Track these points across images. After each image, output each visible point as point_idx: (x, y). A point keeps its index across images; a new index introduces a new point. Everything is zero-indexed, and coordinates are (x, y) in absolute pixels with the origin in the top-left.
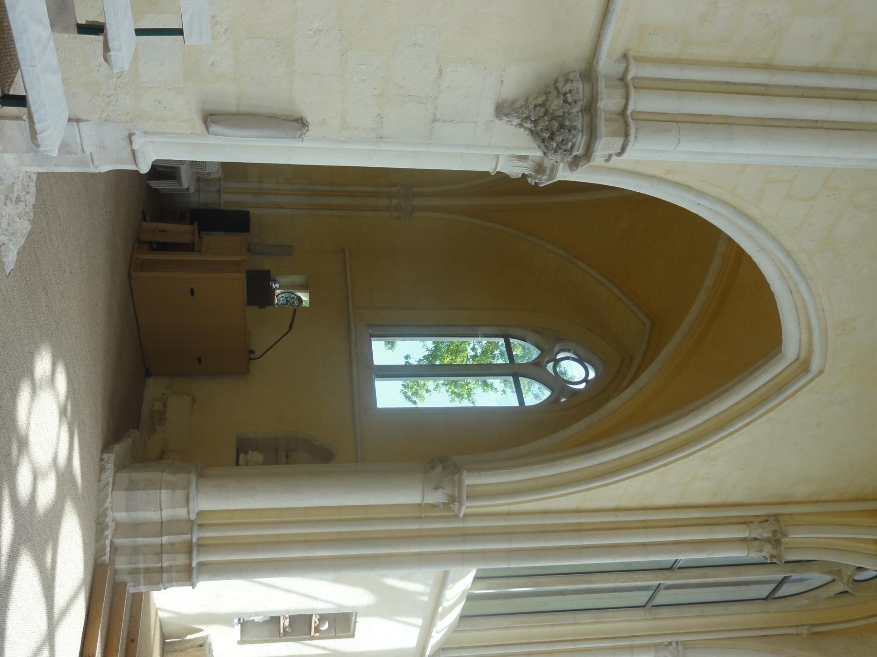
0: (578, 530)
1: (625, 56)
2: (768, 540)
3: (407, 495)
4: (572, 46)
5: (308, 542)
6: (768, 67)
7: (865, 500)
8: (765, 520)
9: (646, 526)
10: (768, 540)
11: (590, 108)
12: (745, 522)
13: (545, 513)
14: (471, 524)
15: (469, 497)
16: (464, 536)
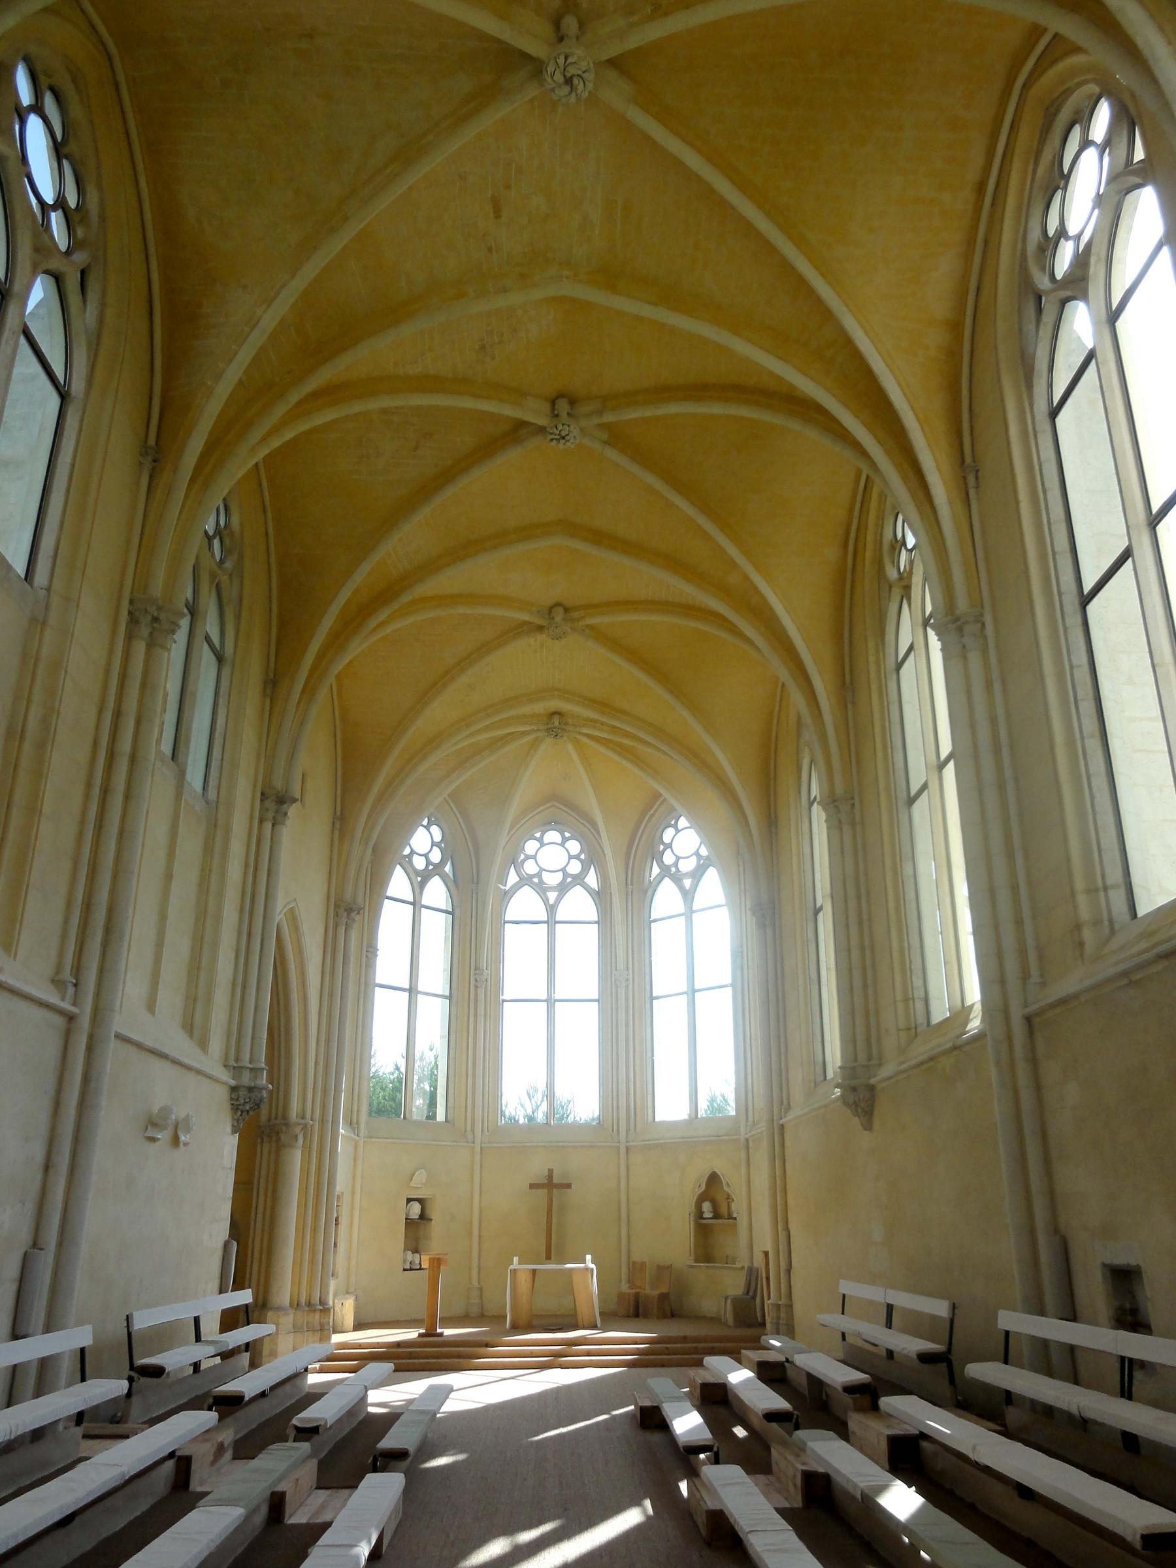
0: (328, 1041)
1: (225, 1066)
2: (348, 915)
3: (295, 1159)
4: (222, 1094)
5: (315, 1230)
6: (234, 985)
7: (332, 840)
8: (337, 915)
9: (331, 995)
10: (348, 915)
11: (250, 1089)
12: (336, 926)
13: (316, 1063)
14: (317, 1115)
15: (303, 1118)
16: (323, 1121)
